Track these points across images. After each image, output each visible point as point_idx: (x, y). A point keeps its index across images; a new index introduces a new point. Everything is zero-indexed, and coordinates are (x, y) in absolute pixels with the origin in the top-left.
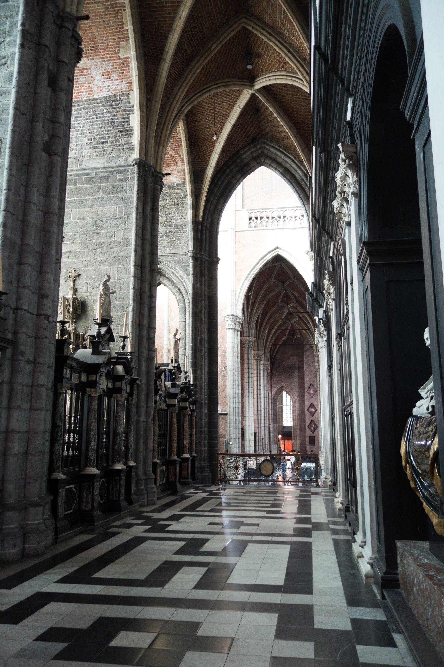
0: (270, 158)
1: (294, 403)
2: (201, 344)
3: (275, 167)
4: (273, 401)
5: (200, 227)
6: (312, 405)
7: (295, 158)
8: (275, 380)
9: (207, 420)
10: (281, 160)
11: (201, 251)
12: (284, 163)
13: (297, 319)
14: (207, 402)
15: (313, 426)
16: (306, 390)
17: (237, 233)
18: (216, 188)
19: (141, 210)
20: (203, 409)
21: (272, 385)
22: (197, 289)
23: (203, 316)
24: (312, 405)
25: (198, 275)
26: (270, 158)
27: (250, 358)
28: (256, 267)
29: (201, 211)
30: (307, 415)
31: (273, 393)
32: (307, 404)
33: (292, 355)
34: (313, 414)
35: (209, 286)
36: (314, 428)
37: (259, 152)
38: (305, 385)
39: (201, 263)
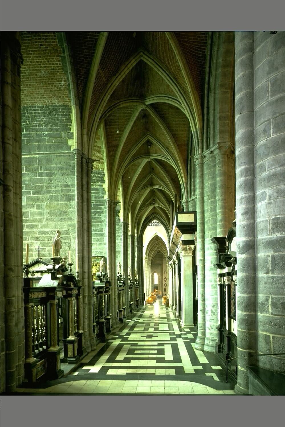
0: (157, 218)
1: (159, 277)
6: (165, 278)
24: (165, 278)
30: (164, 281)
32: (164, 277)
33: (158, 260)
34: (166, 281)
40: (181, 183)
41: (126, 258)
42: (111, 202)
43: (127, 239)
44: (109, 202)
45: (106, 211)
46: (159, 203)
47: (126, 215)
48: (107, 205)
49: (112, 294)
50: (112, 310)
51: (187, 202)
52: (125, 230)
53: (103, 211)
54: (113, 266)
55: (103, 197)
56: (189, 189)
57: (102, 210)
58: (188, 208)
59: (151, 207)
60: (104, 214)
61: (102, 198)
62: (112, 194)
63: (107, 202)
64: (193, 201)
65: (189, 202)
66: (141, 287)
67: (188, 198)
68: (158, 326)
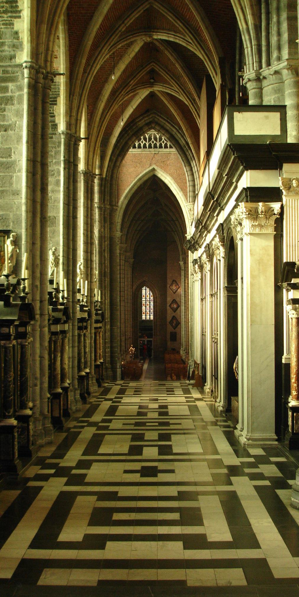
0: (159, 125)
2: (105, 276)
3: (163, 132)
5: (103, 182)
7: (180, 129)
8: (136, 274)
9: (109, 333)
10: (168, 128)
11: (104, 202)
12: (170, 130)
14: (109, 320)
16: (168, 286)
18: (116, 149)
19: (86, 205)
20: (107, 325)
22: (102, 232)
23: (106, 254)
24: (174, 301)
25: (103, 221)
26: (159, 125)
29: (105, 170)
31: (134, 288)
32: (169, 300)
34: (175, 310)
35: (110, 229)
36: (175, 324)
37: (151, 120)
38: (168, 280)
39: (104, 212)
40: (242, 25)
41: (71, 238)
42: (38, 72)
43: (75, 181)
44: (30, 73)
45: (21, 97)
46: (165, 82)
47: (74, 114)
48: (26, 80)
49: (33, 342)
50: (34, 392)
51: (259, 79)
52: (69, 157)
53: (11, 98)
54: (38, 261)
55: (13, 57)
56: (264, 43)
57: (9, 94)
58: (260, 95)
59: (144, 93)
60: (16, 107)
61: (11, 59)
62: (42, 49)
63: (26, 72)
64: (278, 76)
65: (265, 78)
66: (108, 327)
67: (261, 67)
68: (169, 440)
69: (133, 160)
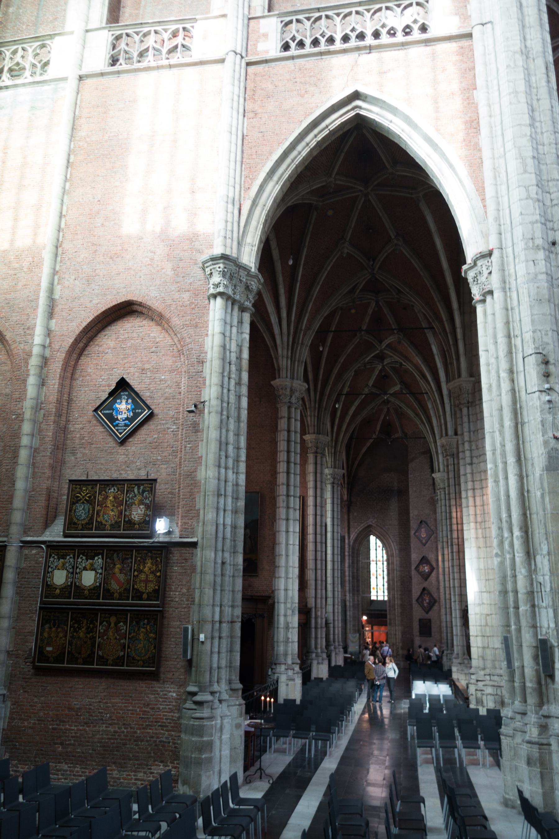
4: (353, 553)
6: (424, 560)
8: (355, 514)
13: (397, 388)
15: (427, 599)
16: (412, 532)
17: (251, 69)
21: (351, 523)
24: (424, 560)
27: (293, 428)
28: (299, 148)
30: (416, 579)
32: (415, 557)
34: (426, 577)
36: (429, 603)
38: (412, 522)
69: (298, 80)
